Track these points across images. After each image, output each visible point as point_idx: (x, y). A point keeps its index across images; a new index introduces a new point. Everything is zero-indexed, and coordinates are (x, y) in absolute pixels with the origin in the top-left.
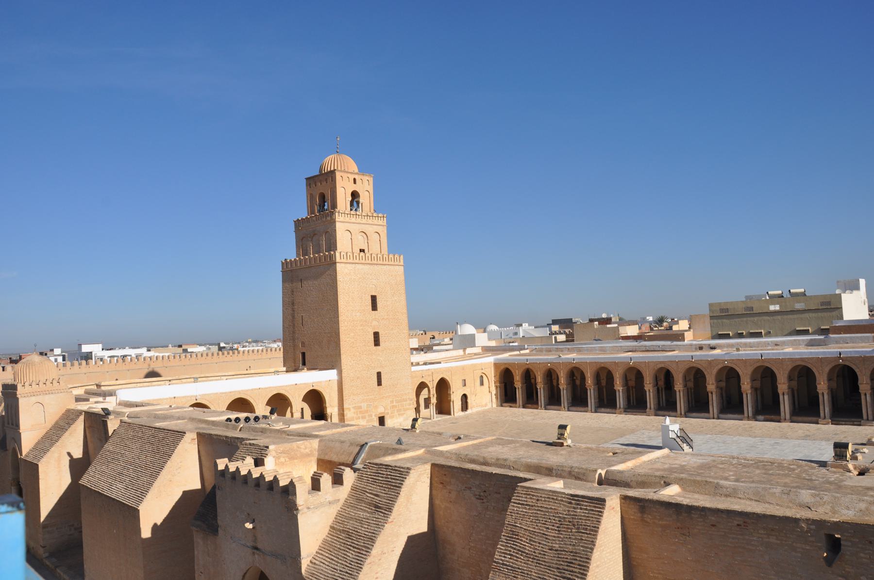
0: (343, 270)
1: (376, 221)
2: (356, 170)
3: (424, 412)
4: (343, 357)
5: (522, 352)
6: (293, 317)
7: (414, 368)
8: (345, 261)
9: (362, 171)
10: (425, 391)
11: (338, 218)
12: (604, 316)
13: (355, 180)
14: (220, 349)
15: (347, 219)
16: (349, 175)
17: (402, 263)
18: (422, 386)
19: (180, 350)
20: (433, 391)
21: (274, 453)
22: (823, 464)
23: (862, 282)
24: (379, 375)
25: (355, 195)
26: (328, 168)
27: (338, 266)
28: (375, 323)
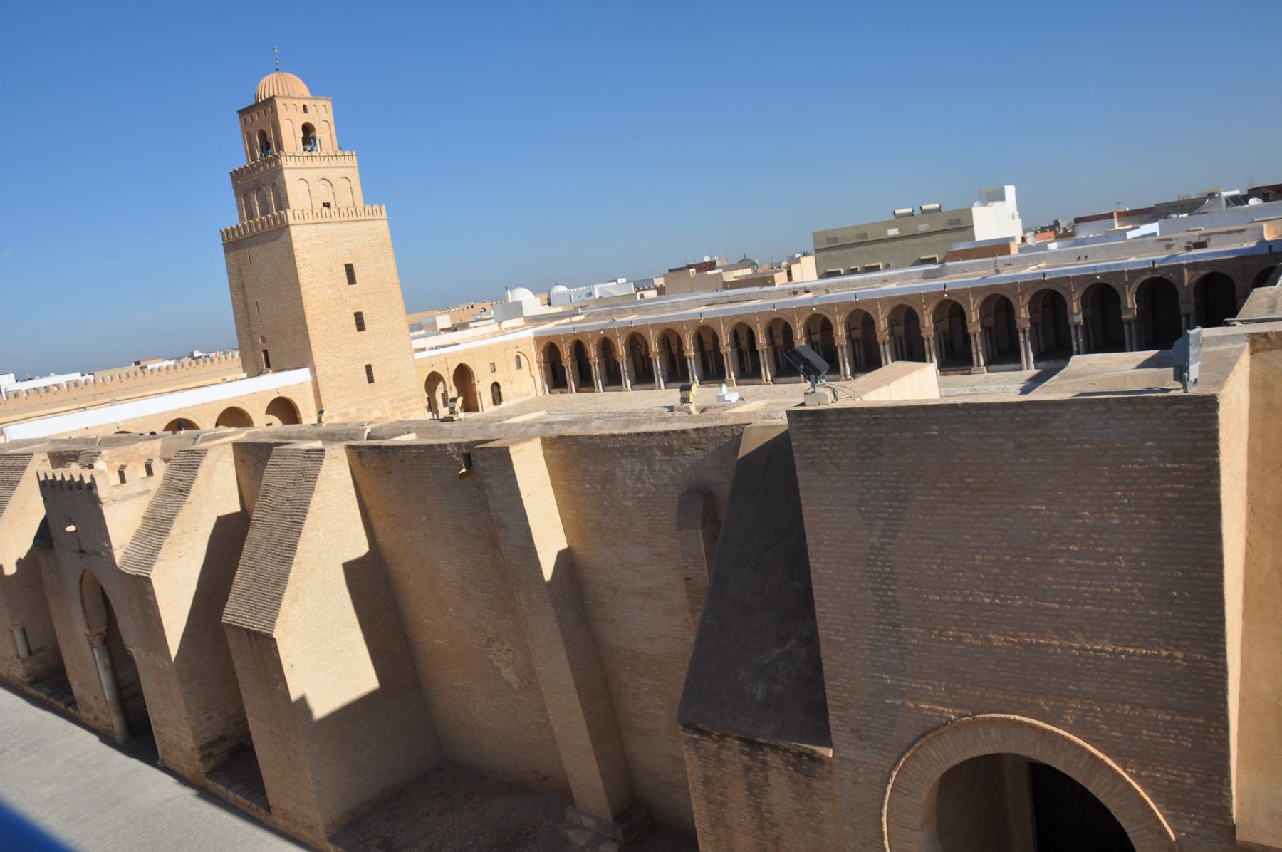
0: (300, 235)
1: (341, 162)
2: (307, 94)
3: (444, 412)
4: (315, 350)
5: (574, 319)
6: (246, 304)
7: (418, 356)
8: (301, 221)
9: (316, 93)
10: (441, 385)
11: (286, 163)
12: (707, 259)
13: (305, 107)
14: (194, 358)
15: (300, 164)
16: (296, 102)
17: (385, 215)
18: (433, 380)
19: (138, 367)
20: (450, 382)
21: (107, 458)
22: (671, 409)
23: (1010, 191)
24: (369, 368)
25: (307, 129)
26: (265, 95)
27: (293, 230)
28: (355, 301)
